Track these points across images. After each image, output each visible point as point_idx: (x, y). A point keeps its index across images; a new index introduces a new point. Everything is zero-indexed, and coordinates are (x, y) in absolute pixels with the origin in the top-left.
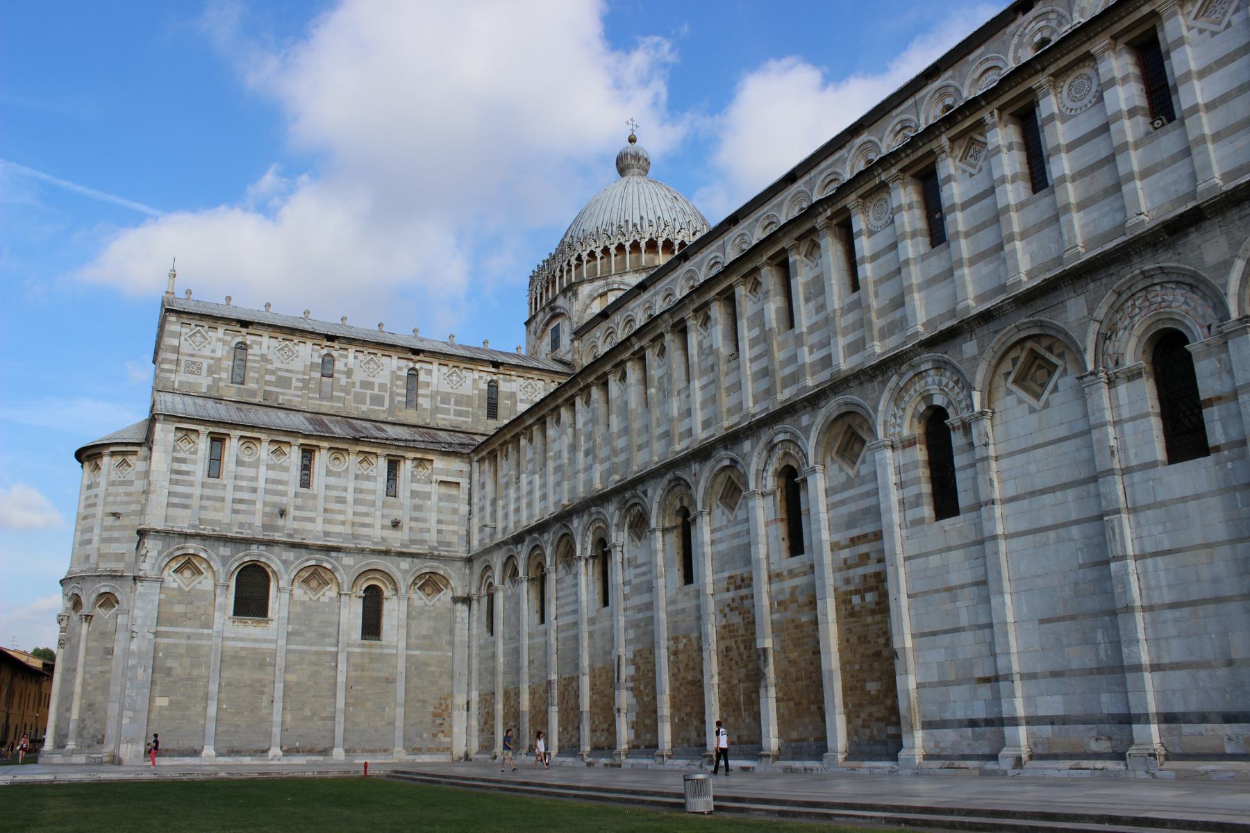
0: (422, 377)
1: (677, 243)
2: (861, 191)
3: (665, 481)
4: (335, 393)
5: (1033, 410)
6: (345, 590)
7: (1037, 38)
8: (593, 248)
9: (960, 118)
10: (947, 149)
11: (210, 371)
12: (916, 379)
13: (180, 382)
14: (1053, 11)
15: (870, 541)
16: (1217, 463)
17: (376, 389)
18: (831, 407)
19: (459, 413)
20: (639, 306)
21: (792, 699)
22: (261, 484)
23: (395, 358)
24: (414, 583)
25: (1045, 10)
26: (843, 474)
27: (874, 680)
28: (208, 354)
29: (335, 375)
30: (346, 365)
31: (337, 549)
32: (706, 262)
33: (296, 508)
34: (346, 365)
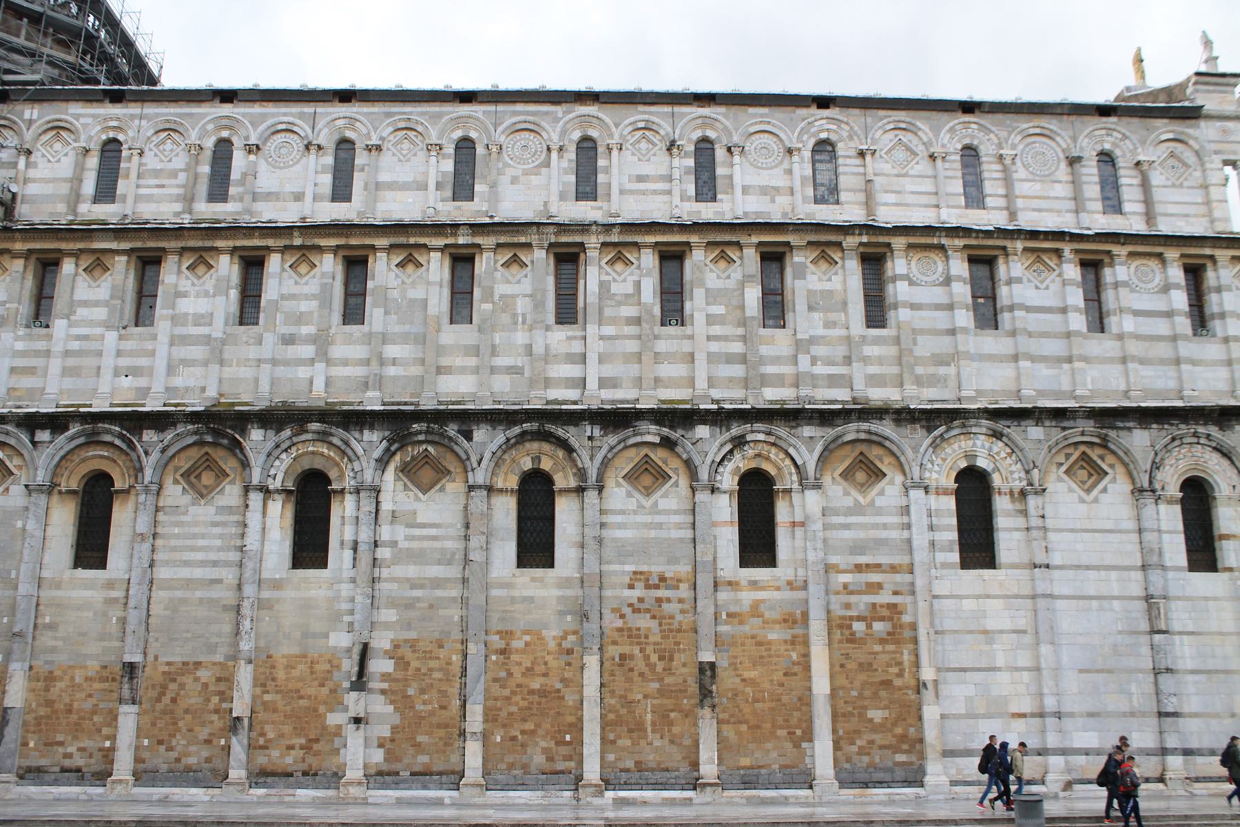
2: (913, 240)
3: (517, 430)
5: (1082, 501)
7: (823, 135)
9: (1042, 237)
10: (1019, 253)
12: (962, 437)
14: (847, 123)
15: (884, 572)
16: (1231, 580)
20: (94, 116)
21: (746, 722)
25: (841, 118)
26: (851, 499)
27: (877, 708)
32: (269, 122)
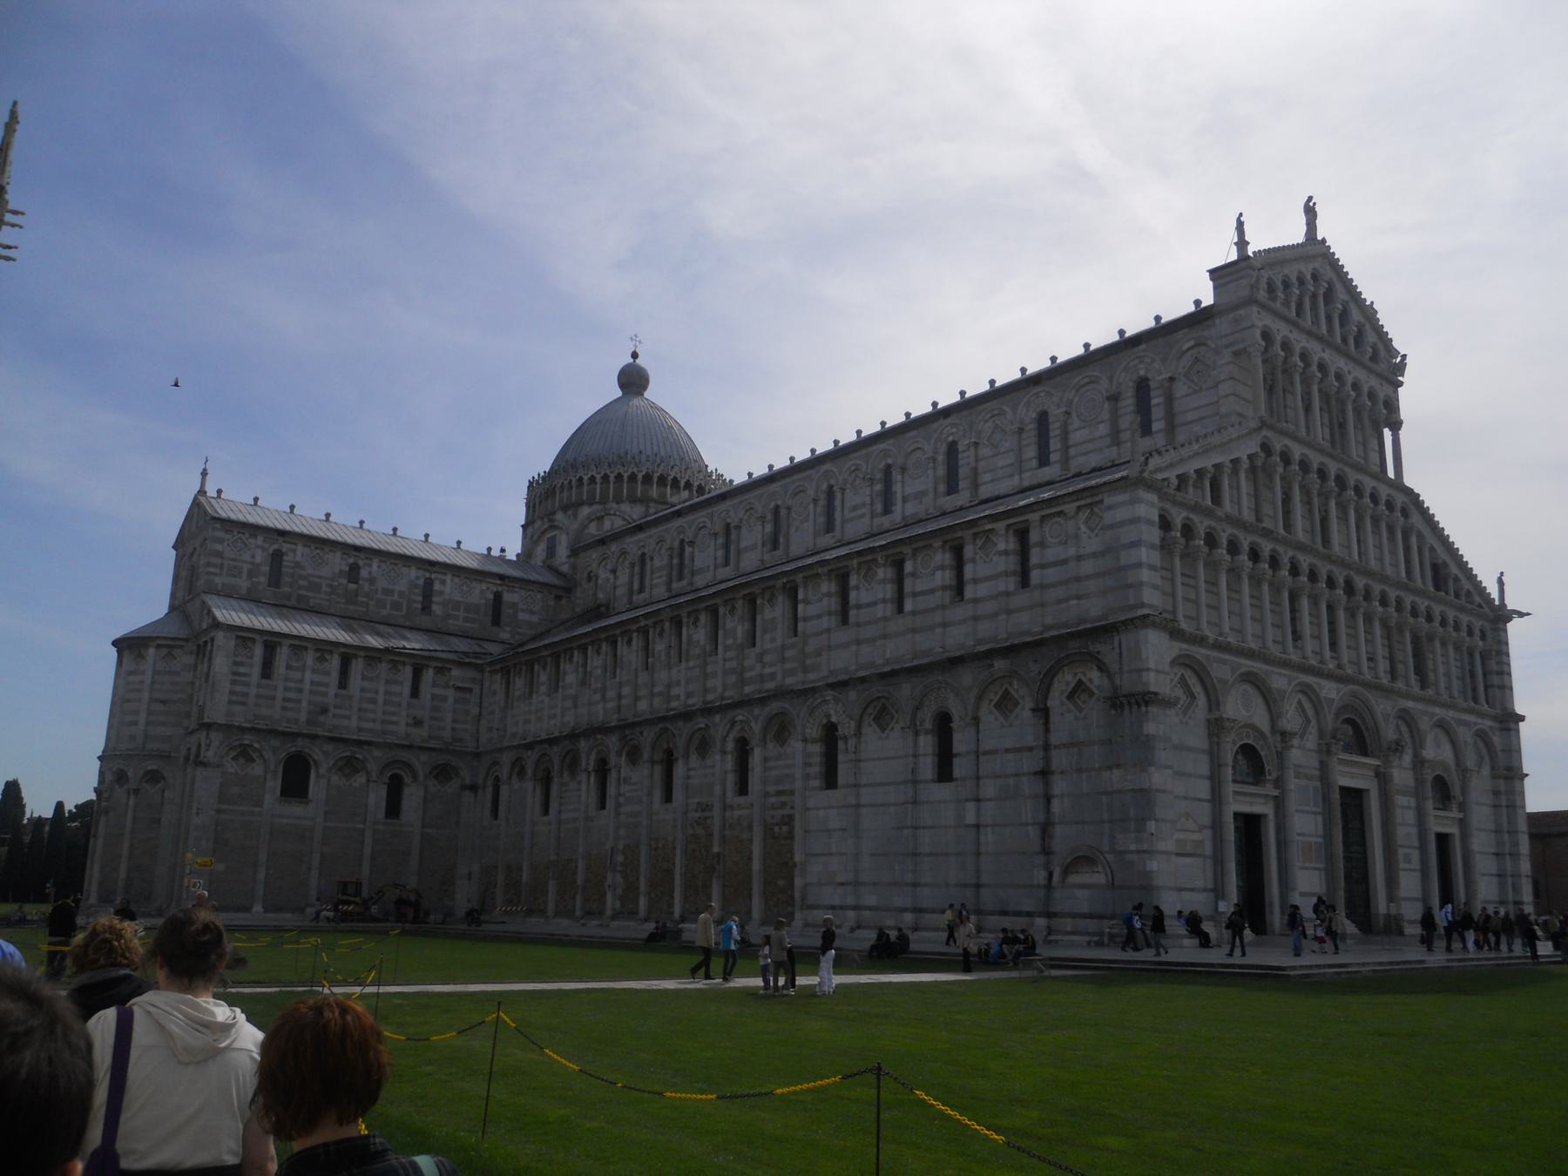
0: (437, 586)
1: (670, 478)
4: (359, 599)
6: (374, 777)
7: (950, 439)
8: (594, 473)
11: (251, 574)
13: (223, 585)
17: (396, 596)
18: (774, 706)
19: (466, 620)
22: (307, 686)
23: (413, 568)
24: (430, 773)
28: (248, 559)
29: (360, 582)
30: (370, 573)
31: (369, 743)
33: (336, 707)
34: (370, 573)
